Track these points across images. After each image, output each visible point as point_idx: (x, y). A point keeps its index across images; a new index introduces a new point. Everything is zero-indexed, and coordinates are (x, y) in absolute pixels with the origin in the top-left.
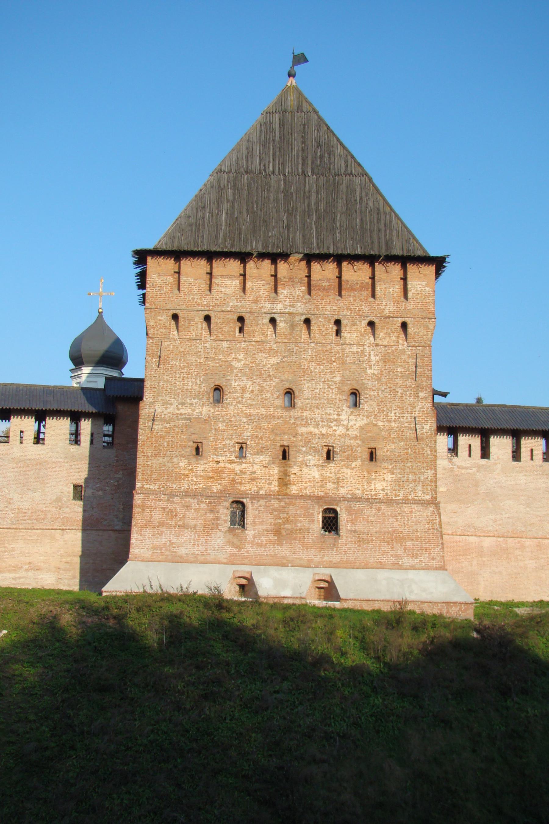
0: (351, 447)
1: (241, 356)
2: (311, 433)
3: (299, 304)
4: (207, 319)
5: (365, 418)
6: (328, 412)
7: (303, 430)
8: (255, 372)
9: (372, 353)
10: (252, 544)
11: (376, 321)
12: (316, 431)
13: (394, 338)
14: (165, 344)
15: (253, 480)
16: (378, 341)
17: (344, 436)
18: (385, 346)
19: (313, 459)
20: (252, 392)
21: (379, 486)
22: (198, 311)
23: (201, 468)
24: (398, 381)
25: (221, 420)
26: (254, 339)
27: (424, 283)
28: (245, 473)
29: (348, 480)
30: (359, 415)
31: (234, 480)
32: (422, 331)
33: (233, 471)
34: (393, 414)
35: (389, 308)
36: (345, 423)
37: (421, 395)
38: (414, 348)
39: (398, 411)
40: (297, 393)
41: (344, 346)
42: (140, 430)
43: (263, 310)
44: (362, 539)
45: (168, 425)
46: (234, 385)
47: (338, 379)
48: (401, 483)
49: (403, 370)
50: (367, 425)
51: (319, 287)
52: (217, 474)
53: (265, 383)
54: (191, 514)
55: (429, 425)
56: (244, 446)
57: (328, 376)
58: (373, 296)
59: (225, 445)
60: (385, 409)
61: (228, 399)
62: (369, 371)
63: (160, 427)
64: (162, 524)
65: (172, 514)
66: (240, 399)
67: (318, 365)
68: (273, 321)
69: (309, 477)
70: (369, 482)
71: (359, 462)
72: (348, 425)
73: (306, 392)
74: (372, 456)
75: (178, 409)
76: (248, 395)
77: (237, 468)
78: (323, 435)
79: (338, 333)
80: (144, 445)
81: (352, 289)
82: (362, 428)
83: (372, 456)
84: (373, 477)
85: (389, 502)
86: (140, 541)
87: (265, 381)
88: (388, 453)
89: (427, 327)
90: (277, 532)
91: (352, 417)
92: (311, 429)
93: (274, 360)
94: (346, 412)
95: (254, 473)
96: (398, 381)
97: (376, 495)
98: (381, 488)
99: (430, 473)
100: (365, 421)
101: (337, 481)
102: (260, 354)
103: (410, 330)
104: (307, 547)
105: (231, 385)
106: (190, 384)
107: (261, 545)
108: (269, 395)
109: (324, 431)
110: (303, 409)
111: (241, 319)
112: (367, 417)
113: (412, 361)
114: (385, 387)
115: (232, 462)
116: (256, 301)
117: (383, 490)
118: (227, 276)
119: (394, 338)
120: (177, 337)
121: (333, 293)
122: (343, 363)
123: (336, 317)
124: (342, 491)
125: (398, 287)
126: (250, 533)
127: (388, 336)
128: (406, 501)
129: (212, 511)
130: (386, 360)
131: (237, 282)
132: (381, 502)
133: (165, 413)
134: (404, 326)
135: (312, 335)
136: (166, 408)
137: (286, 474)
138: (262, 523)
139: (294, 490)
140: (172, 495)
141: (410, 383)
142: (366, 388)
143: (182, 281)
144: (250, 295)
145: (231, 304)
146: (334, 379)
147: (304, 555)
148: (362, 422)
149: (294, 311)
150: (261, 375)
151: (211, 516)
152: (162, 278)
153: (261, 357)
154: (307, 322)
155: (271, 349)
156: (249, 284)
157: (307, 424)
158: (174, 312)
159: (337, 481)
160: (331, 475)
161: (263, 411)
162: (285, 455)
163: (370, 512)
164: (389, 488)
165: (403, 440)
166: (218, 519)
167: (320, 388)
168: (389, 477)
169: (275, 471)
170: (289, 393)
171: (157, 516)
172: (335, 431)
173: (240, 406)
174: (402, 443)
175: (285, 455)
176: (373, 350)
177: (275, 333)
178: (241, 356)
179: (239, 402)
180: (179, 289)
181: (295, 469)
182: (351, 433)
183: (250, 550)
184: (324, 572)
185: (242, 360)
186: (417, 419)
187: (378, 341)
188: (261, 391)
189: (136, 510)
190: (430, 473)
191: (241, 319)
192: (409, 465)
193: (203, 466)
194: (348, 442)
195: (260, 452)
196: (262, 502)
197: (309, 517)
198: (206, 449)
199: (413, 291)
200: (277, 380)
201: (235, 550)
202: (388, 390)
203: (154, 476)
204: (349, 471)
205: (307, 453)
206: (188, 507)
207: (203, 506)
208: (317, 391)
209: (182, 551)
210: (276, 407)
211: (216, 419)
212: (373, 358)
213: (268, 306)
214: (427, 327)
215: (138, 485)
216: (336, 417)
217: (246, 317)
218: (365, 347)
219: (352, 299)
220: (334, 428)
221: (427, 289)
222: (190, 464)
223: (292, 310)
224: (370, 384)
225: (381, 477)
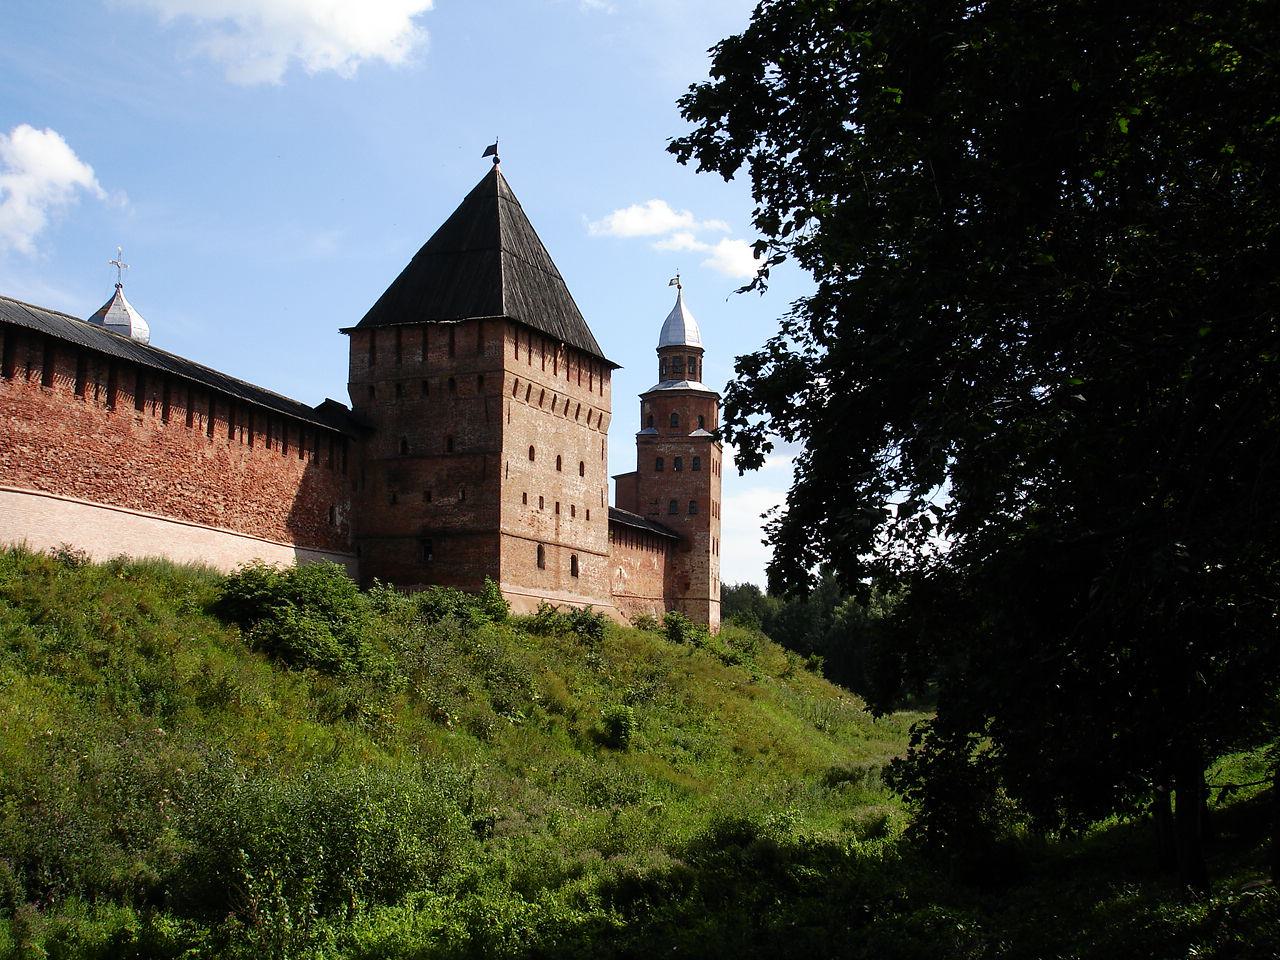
21: (590, 539)
46: (539, 447)
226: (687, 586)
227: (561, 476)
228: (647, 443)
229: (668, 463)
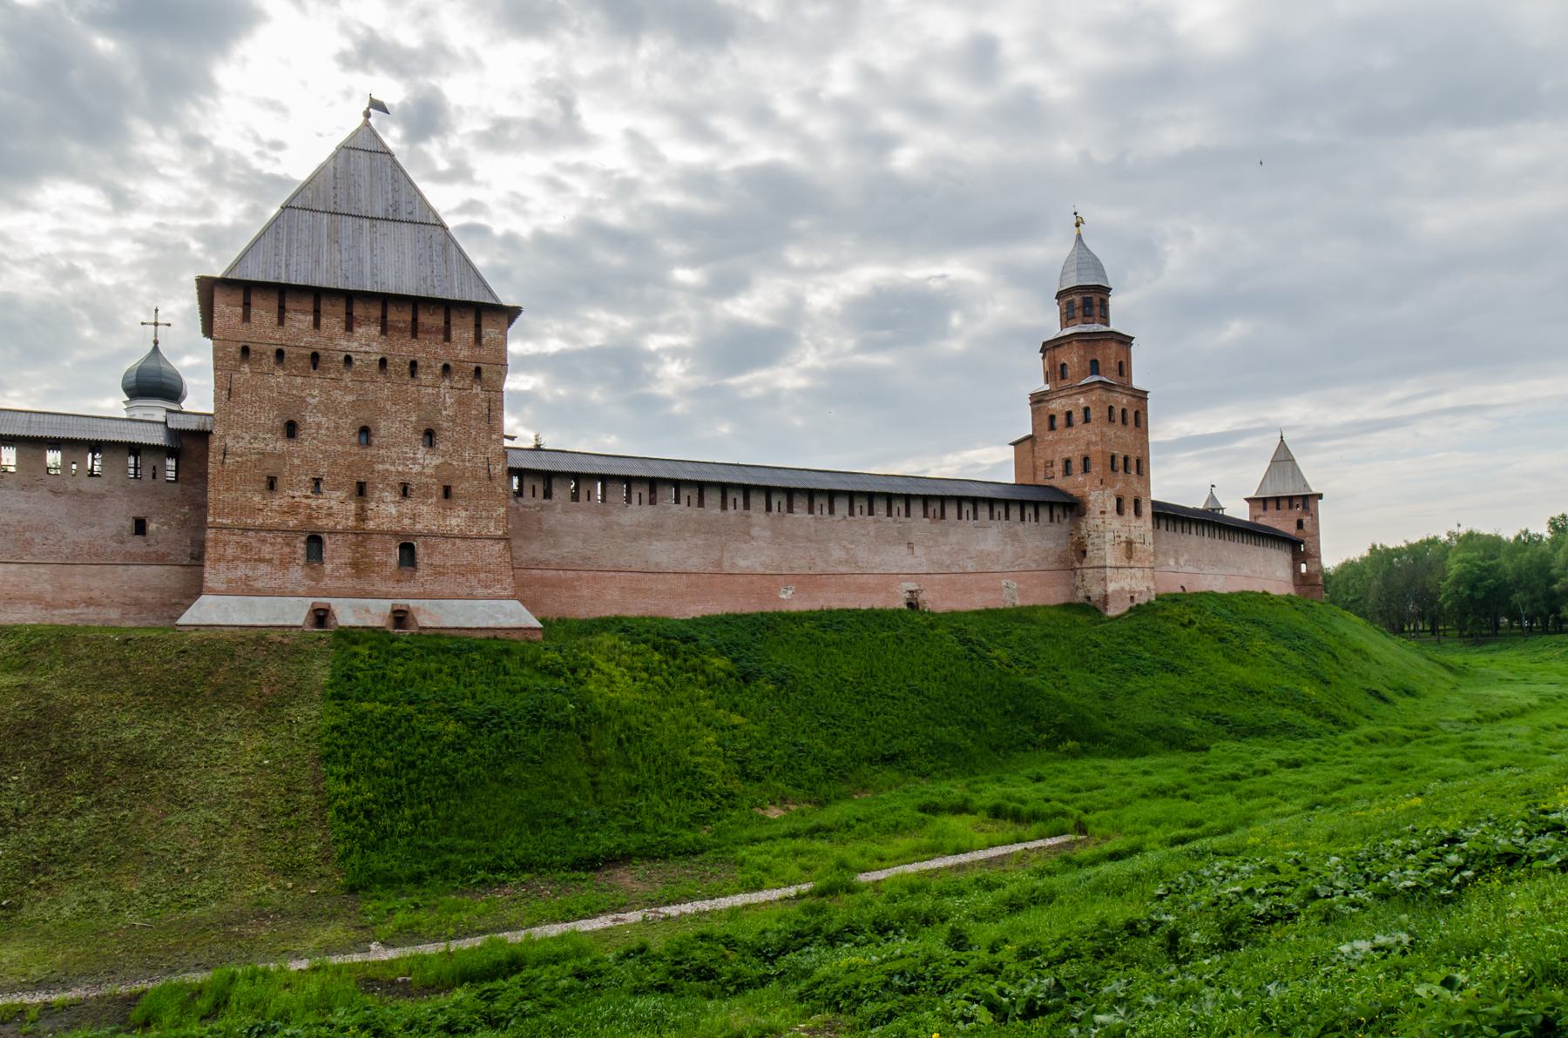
0: (427, 485)
7: (380, 467)
8: (329, 408)
10: (331, 576)
12: (392, 469)
14: (236, 376)
17: (421, 474)
19: (389, 496)
21: (454, 522)
23: (276, 503)
29: (425, 516)
33: (309, 506)
35: (464, 353)
44: (439, 572)
47: (414, 419)
52: (293, 510)
57: (404, 416)
58: (448, 338)
61: (302, 434)
65: (246, 548)
70: (444, 517)
71: (434, 499)
72: (424, 463)
74: (447, 492)
77: (314, 503)
79: (413, 374)
81: (428, 332)
82: (437, 467)
83: (447, 492)
86: (213, 575)
90: (355, 565)
93: (349, 398)
100: (440, 460)
101: (414, 517)
103: (485, 375)
104: (385, 579)
107: (338, 578)
110: (380, 447)
113: (485, 405)
115: (307, 497)
122: (419, 404)
124: (419, 527)
126: (328, 567)
128: (480, 538)
129: (288, 545)
130: (460, 402)
134: (478, 371)
137: (363, 509)
139: (371, 525)
141: (483, 425)
144: (324, 332)
147: (383, 587)
148: (437, 461)
150: (336, 412)
153: (337, 394)
156: (323, 321)
157: (383, 462)
159: (414, 517)
161: (339, 448)
163: (446, 546)
167: (395, 427)
168: (463, 514)
169: (352, 506)
170: (365, 431)
171: (230, 552)
178: (316, 392)
181: (373, 505)
182: (428, 471)
183: (327, 582)
184: (402, 603)
188: (337, 428)
194: (424, 480)
195: (337, 488)
196: (339, 537)
198: (280, 483)
205: (383, 490)
206: (263, 541)
209: (259, 585)
211: (291, 455)
213: (344, 344)
215: (210, 519)
217: (321, 353)
226: (1084, 553)
227: (372, 451)
228: (1039, 402)
229: (1060, 421)
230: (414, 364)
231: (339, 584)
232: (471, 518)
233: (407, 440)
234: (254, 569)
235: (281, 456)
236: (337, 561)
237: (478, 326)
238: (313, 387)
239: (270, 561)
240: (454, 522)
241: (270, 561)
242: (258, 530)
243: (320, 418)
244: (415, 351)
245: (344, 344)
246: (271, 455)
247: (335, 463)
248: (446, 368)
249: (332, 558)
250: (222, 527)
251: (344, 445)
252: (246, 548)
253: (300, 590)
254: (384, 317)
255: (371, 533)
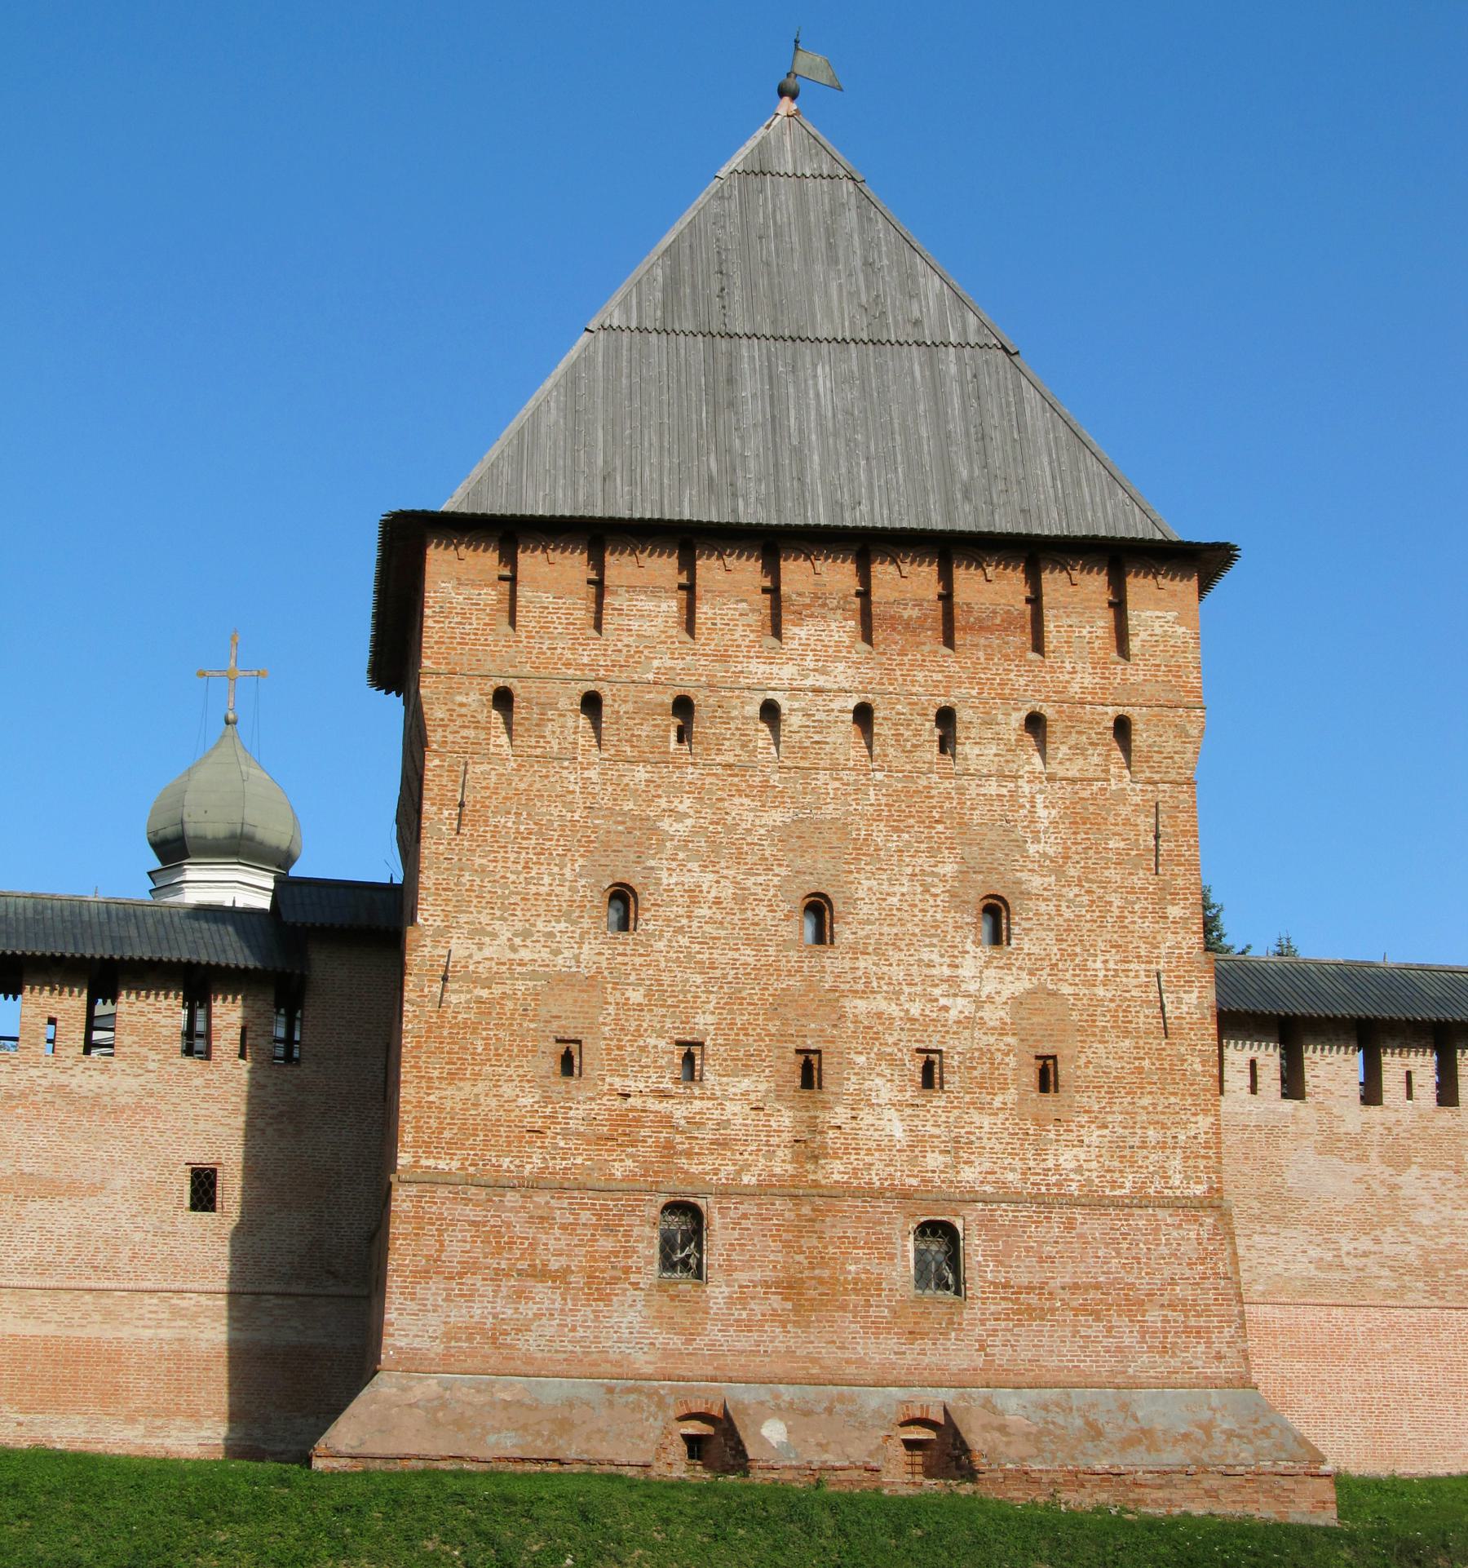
1: (685, 804)
2: (879, 1015)
3: (841, 666)
4: (591, 704)
5: (1024, 974)
6: (926, 957)
8: (722, 844)
9: (1039, 798)
11: (1048, 711)
12: (894, 1010)
13: (1096, 759)
15: (723, 1144)
16: (1054, 767)
17: (967, 1023)
18: (1073, 781)
19: (883, 1089)
20: (717, 902)
21: (1068, 1159)
22: (566, 681)
23: (578, 1112)
24: (1112, 873)
25: (632, 978)
26: (718, 759)
27: (1171, 615)
28: (700, 1125)
30: (1009, 967)
31: (669, 1145)
32: (1171, 744)
33: (667, 1121)
34: (1099, 965)
35: (1083, 680)
36: (972, 987)
37: (1174, 911)
38: (1150, 788)
39: (1113, 956)
40: (838, 907)
41: (964, 781)
42: (406, 1007)
43: (743, 681)
45: (485, 993)
46: (666, 880)
47: (949, 869)
48: (1127, 1152)
49: (1122, 845)
50: (1030, 993)
51: (893, 622)
52: (622, 1130)
53: (753, 879)
54: (553, 1240)
55: (1195, 995)
56: (696, 1050)
57: (922, 861)
58: (1038, 646)
59: (643, 1049)
60: (1078, 950)
61: (647, 922)
62: (1032, 849)
63: (463, 997)
64: (470, 1268)
65: (498, 1240)
66: (684, 921)
67: (896, 830)
68: (770, 712)
69: (876, 1135)
70: (1040, 1153)
71: (1011, 1096)
72: (979, 990)
73: (864, 901)
74: (1047, 1077)
75: (513, 949)
76: (705, 911)
78: (913, 1020)
79: (947, 743)
80: (418, 1046)
81: (981, 627)
82: (1017, 1002)
83: (1047, 1077)
84: (1052, 1135)
85: (1096, 1203)
87: (750, 873)
88: (1091, 1071)
89: (1181, 733)
90: (790, 1287)
91: (990, 973)
92: (881, 1004)
93: (776, 817)
94: (974, 955)
95: (723, 1124)
96: (1112, 873)
97: (1059, 1184)
98: (1073, 1165)
99: (1204, 1122)
100: (1025, 983)
101: (957, 1147)
102: (737, 800)
103: (1141, 738)
104: (876, 1328)
105: (658, 884)
106: (547, 880)
107: (747, 1326)
108: (762, 911)
109: (915, 1011)
111: (683, 707)
112: (1031, 973)
113: (1145, 822)
114: (1076, 890)
115: (663, 1095)
116: (723, 658)
117: (1079, 1170)
118: (644, 590)
119: (1096, 759)
120: (507, 750)
121: (931, 640)
123: (942, 701)
124: (968, 1174)
125: (1103, 622)
126: (717, 1291)
127: (1080, 755)
129: (610, 1230)
131: (671, 606)
132: (1074, 1203)
133: (476, 958)
134: (1122, 728)
135: (877, 750)
136: (480, 947)
137: (814, 1128)
138: (749, 1264)
139: (836, 1171)
140: (498, 1187)
142: (1027, 895)
143: (521, 602)
145: (656, 663)
146: (939, 870)
149: (828, 686)
150: (739, 857)
151: (606, 1244)
152: (467, 591)
153: (741, 808)
154: (863, 715)
155: (765, 785)
156: (703, 610)
157: (867, 992)
158: (501, 682)
159: (957, 1147)
160: (936, 1131)
162: (810, 1073)
164: (1094, 1165)
165: (1127, 1033)
166: (628, 1252)
167: (898, 896)
168: (1094, 1136)
169: (785, 1119)
170: (818, 908)
171: (457, 1248)
172: (946, 1008)
173: (684, 941)
174: (1127, 1042)
175: (810, 1073)
176: (1041, 792)
177: (777, 744)
178: (685, 804)
179: (680, 930)
180: (513, 623)
181: (841, 1114)
185: (686, 815)
186: (1163, 977)
187: (1054, 767)
188: (741, 899)
189: (397, 1228)
190: (1204, 1122)
191: (683, 707)
192: (1146, 1101)
193: (584, 1106)
195: (744, 1066)
197: (880, 1245)
198: (591, 1059)
199: (1143, 635)
200: (783, 871)
201: (677, 1341)
202: (1085, 899)
203: (447, 1134)
204: (986, 1121)
206: (544, 1220)
207: (585, 1216)
208: (894, 900)
209: (530, 1343)
210: (784, 945)
212: (1042, 812)
214: (1181, 733)
215: (404, 1159)
216: (947, 972)
217: (699, 698)
218: (1021, 782)
219: (981, 654)
220: (943, 1001)
221: (1181, 630)
222: (547, 1100)
223: (821, 681)
224: (1036, 882)
225: (1072, 1136)
227: (833, 961)
230: (946, 718)
231: (745, 1342)
232: (1118, 1146)
233: (932, 930)
234: (520, 1295)
235: (592, 983)
236: (743, 1277)
237: (1119, 606)
238: (677, 790)
239: (560, 1277)
240: (1068, 1159)
241: (560, 1277)
242: (531, 1186)
243: (696, 875)
244: (950, 681)
245: (758, 669)
246: (566, 980)
247: (735, 999)
248: (1035, 723)
249: (729, 1269)
250: (435, 1180)
251: (758, 944)
252: (498, 1240)
253: (644, 1362)
254: (865, 595)
255: (835, 1193)
